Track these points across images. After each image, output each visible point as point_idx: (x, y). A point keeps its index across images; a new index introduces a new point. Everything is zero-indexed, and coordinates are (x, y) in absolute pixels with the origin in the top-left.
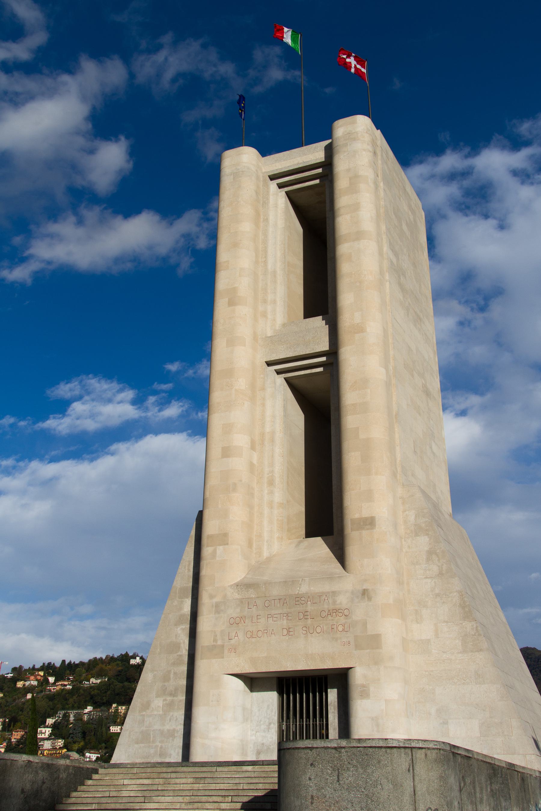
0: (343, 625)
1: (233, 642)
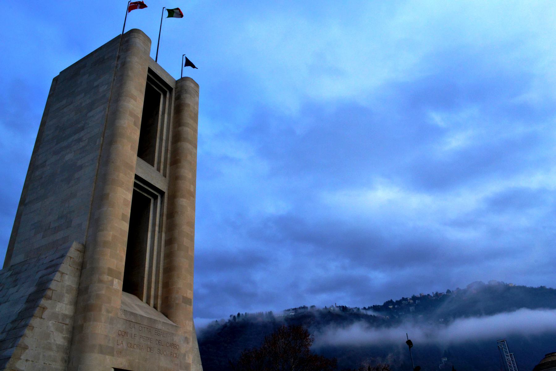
0: (176, 354)
1: (119, 347)
